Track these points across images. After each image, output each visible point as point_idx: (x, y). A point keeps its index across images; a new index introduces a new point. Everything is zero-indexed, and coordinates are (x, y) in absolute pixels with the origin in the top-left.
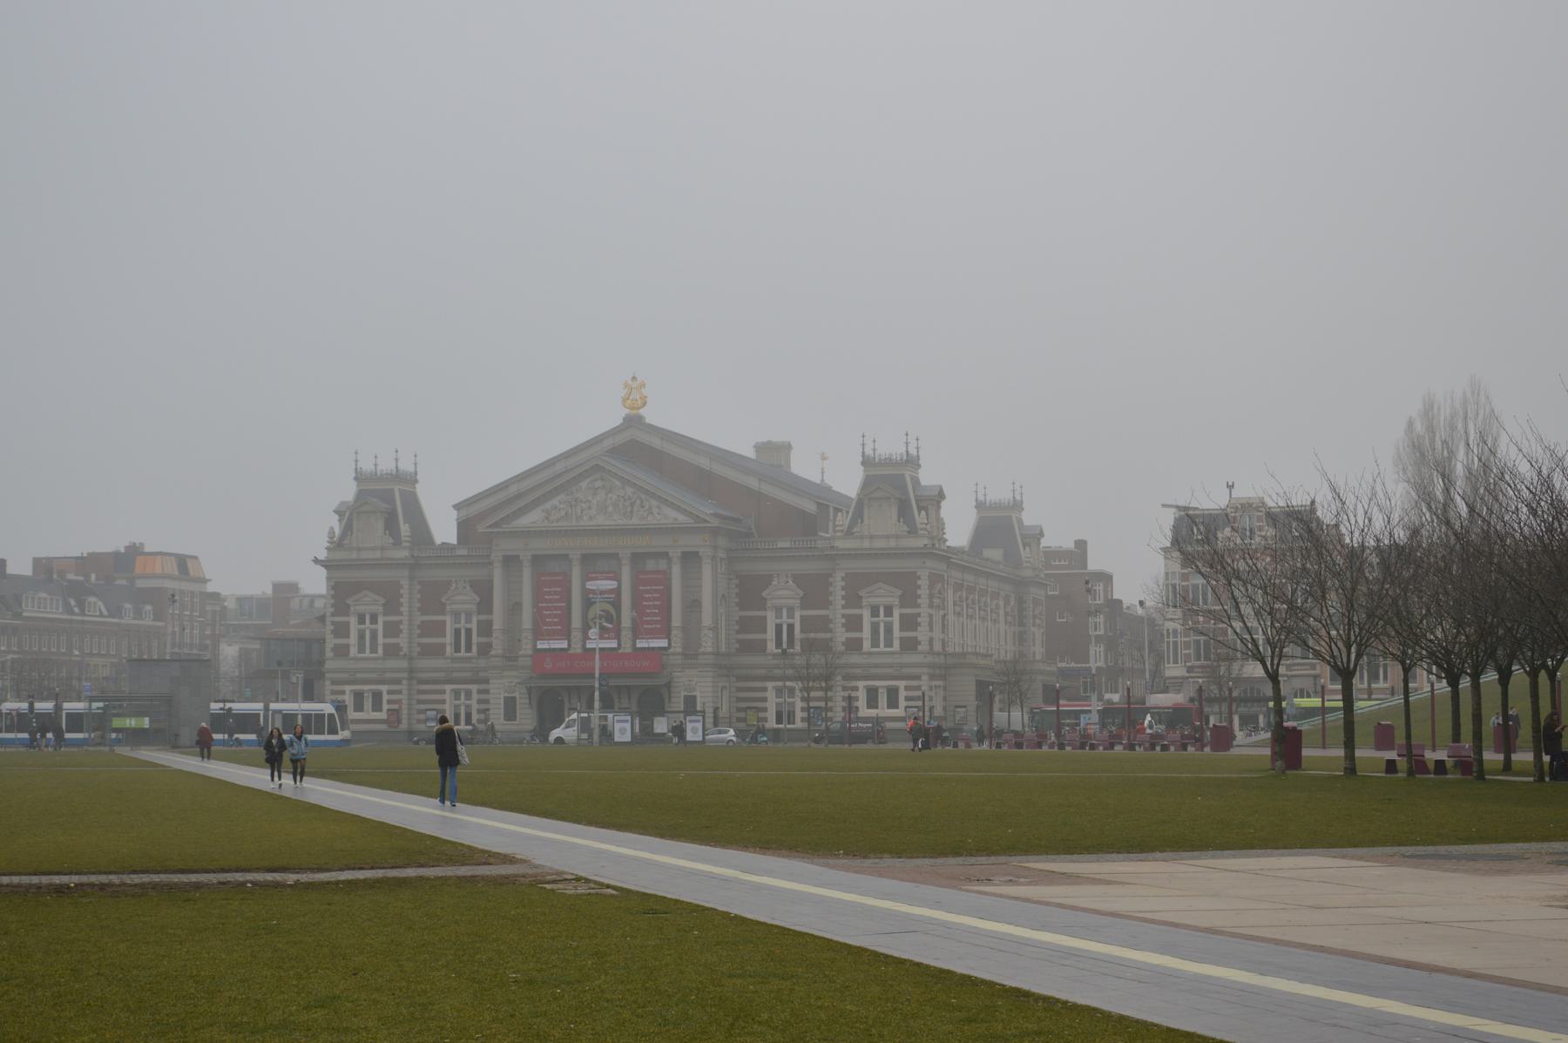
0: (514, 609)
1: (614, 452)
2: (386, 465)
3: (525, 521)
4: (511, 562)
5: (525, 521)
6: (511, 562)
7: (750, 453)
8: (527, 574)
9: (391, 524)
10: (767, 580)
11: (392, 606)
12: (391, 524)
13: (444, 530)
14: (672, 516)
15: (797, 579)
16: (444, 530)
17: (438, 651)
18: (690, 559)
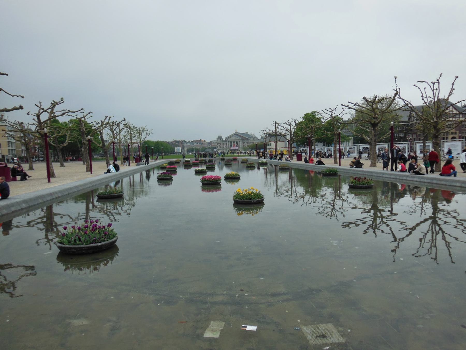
0: (229, 145)
1: (235, 134)
2: (220, 136)
3: (229, 139)
4: (228, 142)
5: (229, 139)
6: (228, 142)
7: (245, 133)
8: (229, 143)
9: (220, 139)
10: (244, 143)
11: (221, 145)
12: (220, 139)
13: (224, 139)
14: (238, 139)
15: (247, 143)
16: (224, 139)
17: (224, 147)
18: (240, 141)
